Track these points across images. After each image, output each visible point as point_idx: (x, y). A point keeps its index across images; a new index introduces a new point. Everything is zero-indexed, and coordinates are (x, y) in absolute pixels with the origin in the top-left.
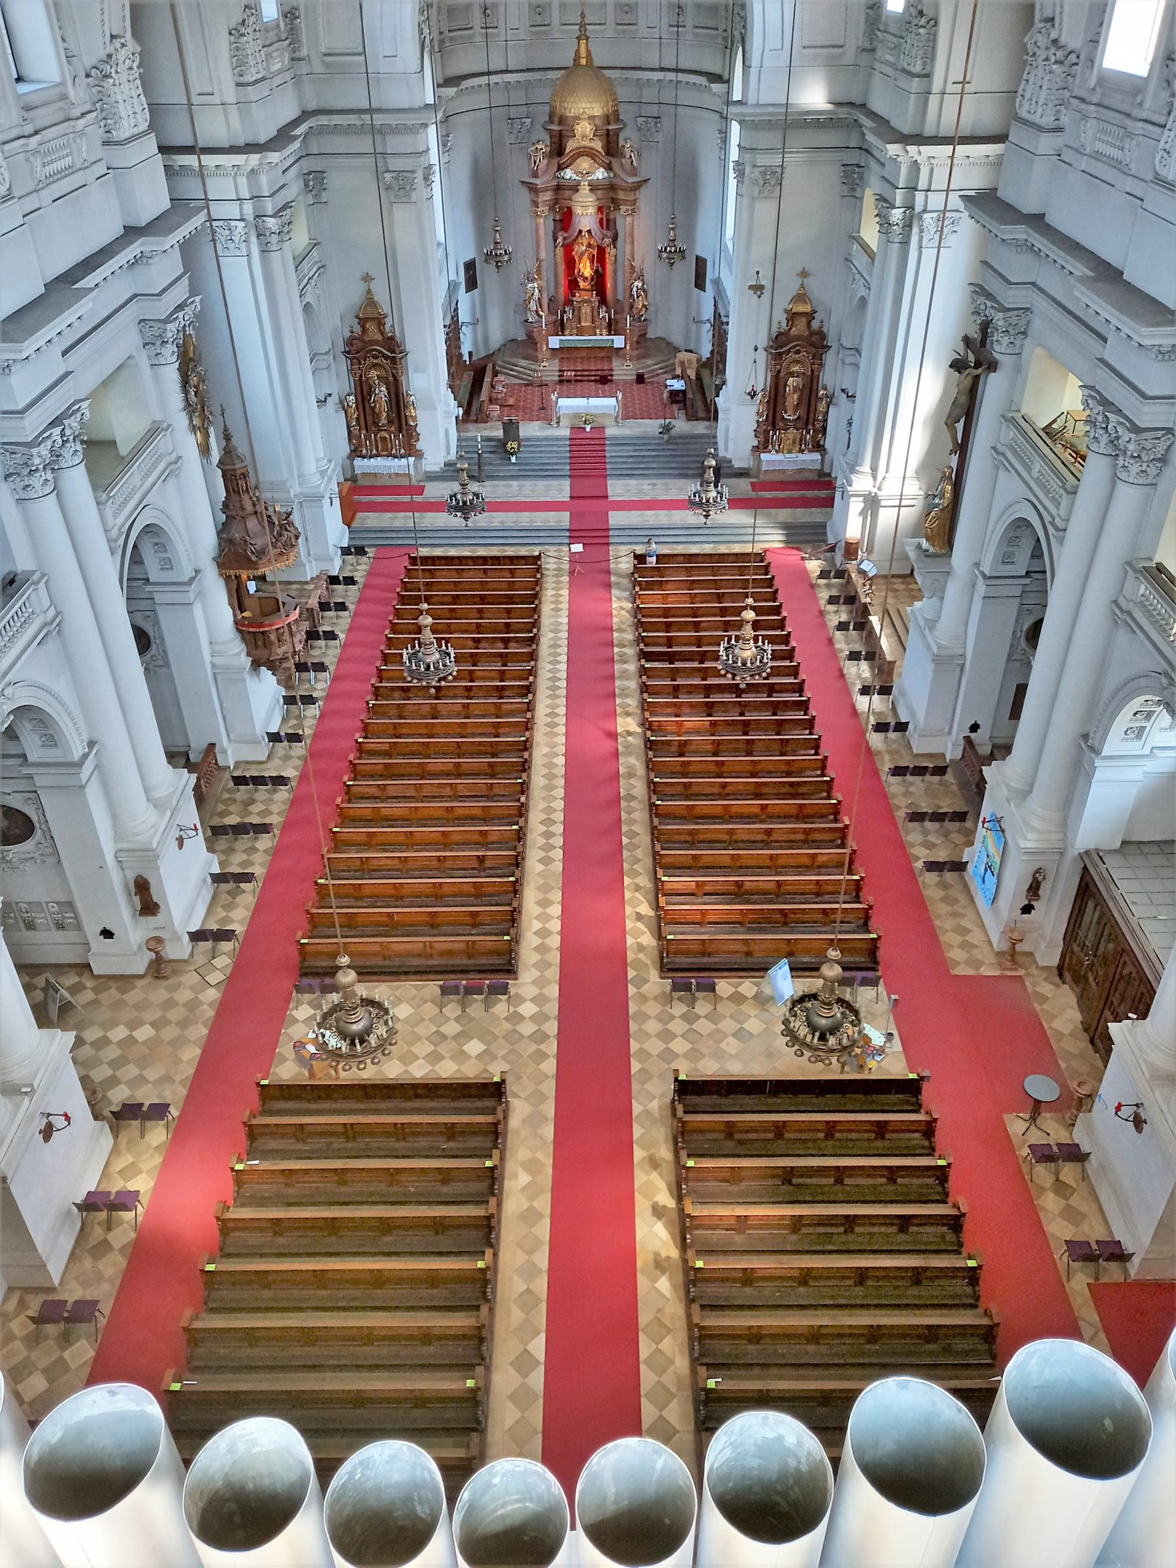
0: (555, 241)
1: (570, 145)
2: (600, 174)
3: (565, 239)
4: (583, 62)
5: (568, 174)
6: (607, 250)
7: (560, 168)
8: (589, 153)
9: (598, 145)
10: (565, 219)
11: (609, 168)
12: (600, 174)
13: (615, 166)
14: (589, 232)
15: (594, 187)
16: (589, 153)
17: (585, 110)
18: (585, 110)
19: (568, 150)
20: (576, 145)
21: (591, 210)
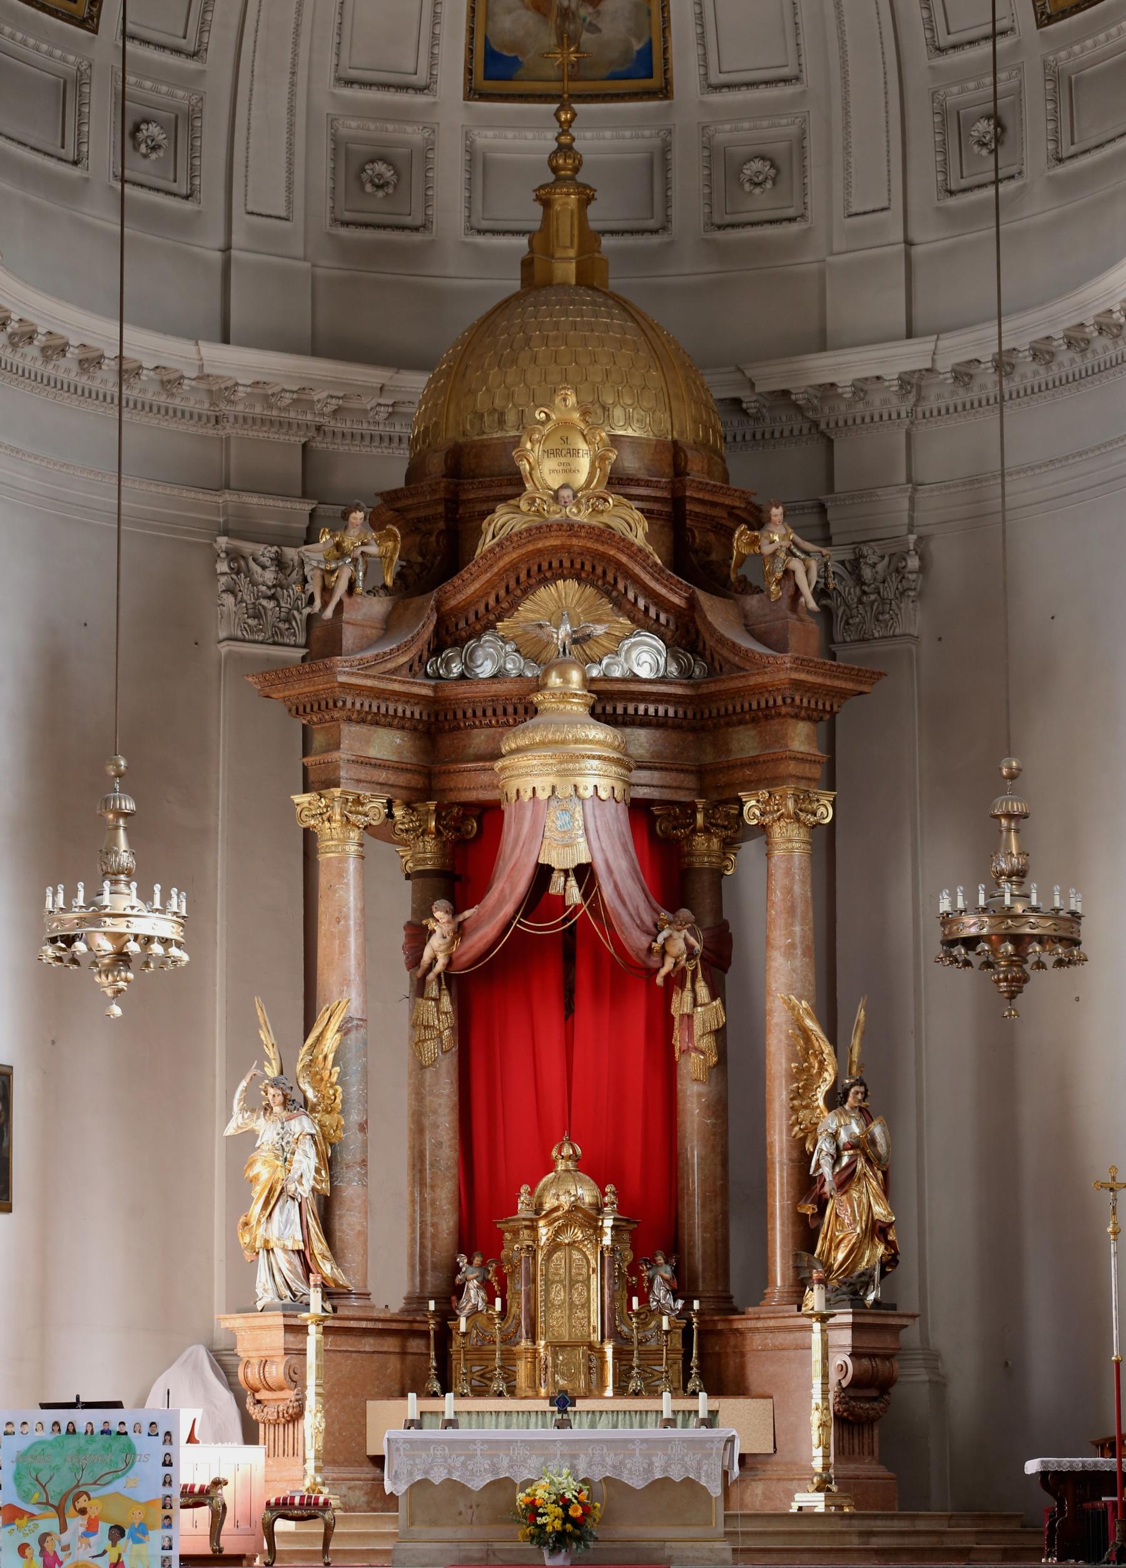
0: (414, 960)
1: (503, 522)
2: (644, 658)
3: (460, 931)
4: (566, 270)
5: (491, 660)
6: (681, 1003)
7: (451, 635)
8: (592, 563)
9: (633, 525)
10: (463, 845)
11: (685, 636)
12: (644, 658)
13: (717, 615)
14: (584, 874)
15: (610, 704)
16: (592, 563)
17: (568, 461)
18: (568, 461)
19: (487, 542)
20: (518, 523)
21: (597, 779)
